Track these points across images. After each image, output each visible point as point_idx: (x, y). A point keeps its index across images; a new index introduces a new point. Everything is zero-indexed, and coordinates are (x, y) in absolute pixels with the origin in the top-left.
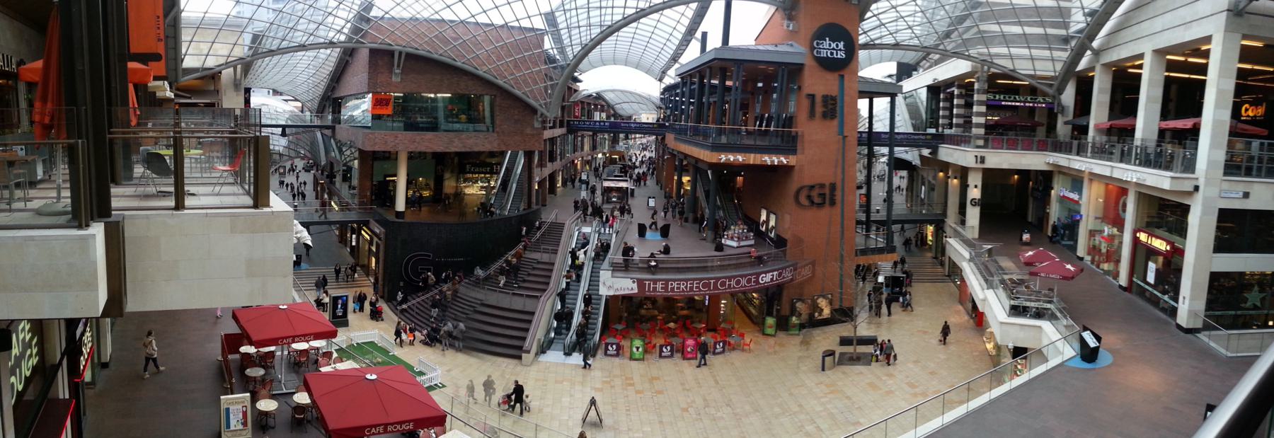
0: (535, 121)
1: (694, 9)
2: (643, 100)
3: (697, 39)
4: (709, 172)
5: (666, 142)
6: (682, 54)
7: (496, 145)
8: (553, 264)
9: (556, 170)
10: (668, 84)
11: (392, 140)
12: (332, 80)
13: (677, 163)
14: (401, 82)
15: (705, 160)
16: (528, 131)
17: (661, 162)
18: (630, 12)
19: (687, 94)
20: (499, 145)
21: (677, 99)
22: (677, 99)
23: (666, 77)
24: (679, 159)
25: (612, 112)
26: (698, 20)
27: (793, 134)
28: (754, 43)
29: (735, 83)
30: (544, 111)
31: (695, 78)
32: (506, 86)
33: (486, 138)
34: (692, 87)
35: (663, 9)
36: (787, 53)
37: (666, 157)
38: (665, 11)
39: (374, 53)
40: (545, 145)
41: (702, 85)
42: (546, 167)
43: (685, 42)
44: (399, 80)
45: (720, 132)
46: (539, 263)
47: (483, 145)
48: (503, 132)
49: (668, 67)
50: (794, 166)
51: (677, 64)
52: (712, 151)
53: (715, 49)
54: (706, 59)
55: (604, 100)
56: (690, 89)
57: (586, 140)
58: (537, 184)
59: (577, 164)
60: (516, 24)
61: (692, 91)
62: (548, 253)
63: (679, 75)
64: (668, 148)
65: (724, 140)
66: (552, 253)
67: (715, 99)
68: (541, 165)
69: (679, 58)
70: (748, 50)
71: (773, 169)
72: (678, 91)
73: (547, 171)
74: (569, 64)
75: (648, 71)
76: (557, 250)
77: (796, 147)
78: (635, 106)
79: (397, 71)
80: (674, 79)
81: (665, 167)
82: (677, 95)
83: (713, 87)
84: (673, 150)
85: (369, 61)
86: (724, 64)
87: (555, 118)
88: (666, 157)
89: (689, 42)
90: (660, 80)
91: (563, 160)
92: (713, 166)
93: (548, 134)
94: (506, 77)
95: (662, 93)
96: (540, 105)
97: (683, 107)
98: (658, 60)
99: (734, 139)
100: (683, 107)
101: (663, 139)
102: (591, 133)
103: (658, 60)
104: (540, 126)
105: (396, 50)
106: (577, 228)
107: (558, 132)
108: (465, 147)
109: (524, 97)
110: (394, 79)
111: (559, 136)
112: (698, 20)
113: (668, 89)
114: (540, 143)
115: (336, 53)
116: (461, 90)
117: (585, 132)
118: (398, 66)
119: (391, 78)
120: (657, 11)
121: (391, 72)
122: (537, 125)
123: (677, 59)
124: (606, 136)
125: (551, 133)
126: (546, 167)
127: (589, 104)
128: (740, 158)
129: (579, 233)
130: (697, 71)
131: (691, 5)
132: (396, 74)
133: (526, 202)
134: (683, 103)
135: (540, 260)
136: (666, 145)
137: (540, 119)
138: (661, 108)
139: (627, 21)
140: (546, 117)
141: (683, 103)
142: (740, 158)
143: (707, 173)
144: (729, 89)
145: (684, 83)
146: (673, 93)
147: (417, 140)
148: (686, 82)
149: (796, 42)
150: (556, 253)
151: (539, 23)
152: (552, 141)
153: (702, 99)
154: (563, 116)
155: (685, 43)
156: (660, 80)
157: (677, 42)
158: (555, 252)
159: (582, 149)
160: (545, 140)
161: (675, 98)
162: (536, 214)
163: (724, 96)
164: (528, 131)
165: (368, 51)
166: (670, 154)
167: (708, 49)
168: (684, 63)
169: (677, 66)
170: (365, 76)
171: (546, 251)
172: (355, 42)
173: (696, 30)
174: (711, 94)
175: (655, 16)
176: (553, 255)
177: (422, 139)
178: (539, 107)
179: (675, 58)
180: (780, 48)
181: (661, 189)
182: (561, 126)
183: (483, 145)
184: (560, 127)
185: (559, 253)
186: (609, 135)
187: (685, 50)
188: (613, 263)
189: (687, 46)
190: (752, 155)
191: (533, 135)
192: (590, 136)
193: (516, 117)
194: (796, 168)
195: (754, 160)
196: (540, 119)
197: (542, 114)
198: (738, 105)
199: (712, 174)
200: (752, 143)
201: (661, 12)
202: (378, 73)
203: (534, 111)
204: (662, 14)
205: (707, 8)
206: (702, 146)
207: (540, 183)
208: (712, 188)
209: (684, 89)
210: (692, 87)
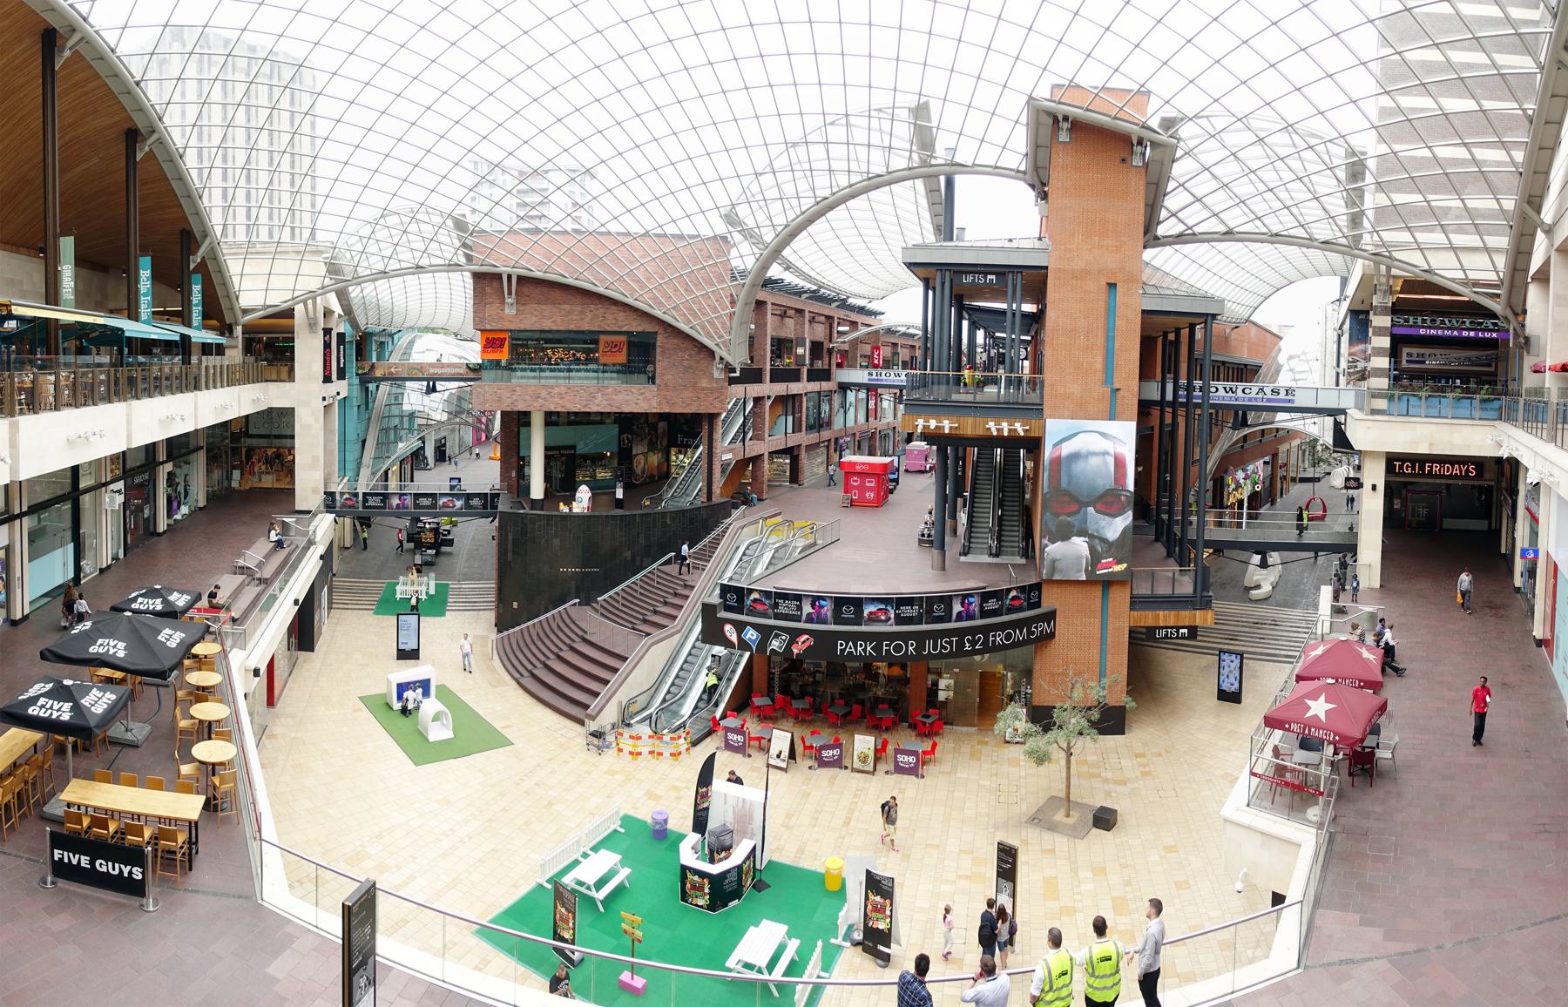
7: (655, 405)
11: (508, 395)
16: (704, 383)
30: (725, 354)
33: (642, 394)
47: (636, 404)
48: (666, 385)
60: (659, 231)
105: (505, 272)
110: (507, 310)
116: (608, 325)
118: (510, 293)
119: (503, 310)
121: (503, 302)
135: (687, 583)
147: (543, 395)
164: (704, 383)
177: (549, 393)
183: (636, 404)
191: (711, 390)
193: (686, 363)
197: (721, 359)
203: (711, 353)
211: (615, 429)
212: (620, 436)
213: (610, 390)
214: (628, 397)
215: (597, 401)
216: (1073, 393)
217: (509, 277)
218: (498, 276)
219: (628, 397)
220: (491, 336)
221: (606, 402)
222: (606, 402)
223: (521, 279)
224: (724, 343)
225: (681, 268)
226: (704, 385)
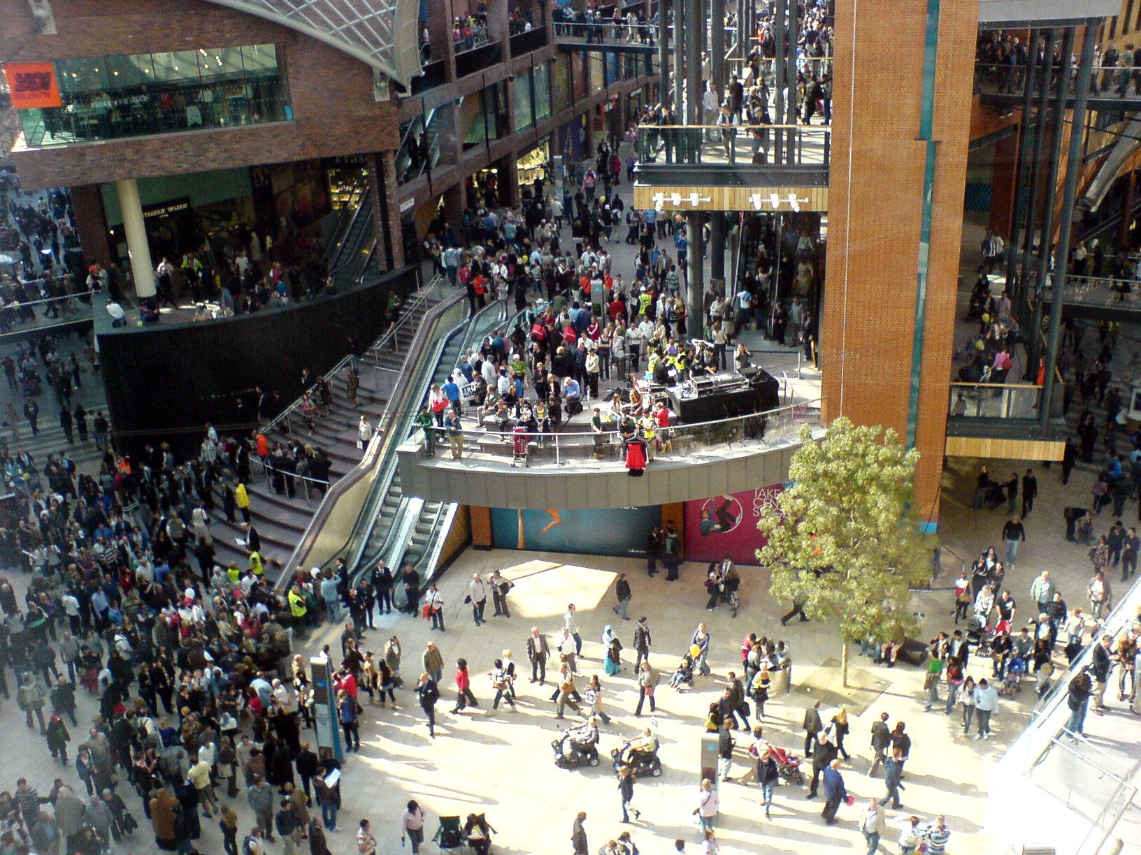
20: (303, 147)
33: (275, 136)
47: (269, 151)
96: (374, 56)
104: (387, 98)
137: (383, 84)
213: (227, 137)
215: (211, 155)
221: (224, 156)
222: (224, 156)
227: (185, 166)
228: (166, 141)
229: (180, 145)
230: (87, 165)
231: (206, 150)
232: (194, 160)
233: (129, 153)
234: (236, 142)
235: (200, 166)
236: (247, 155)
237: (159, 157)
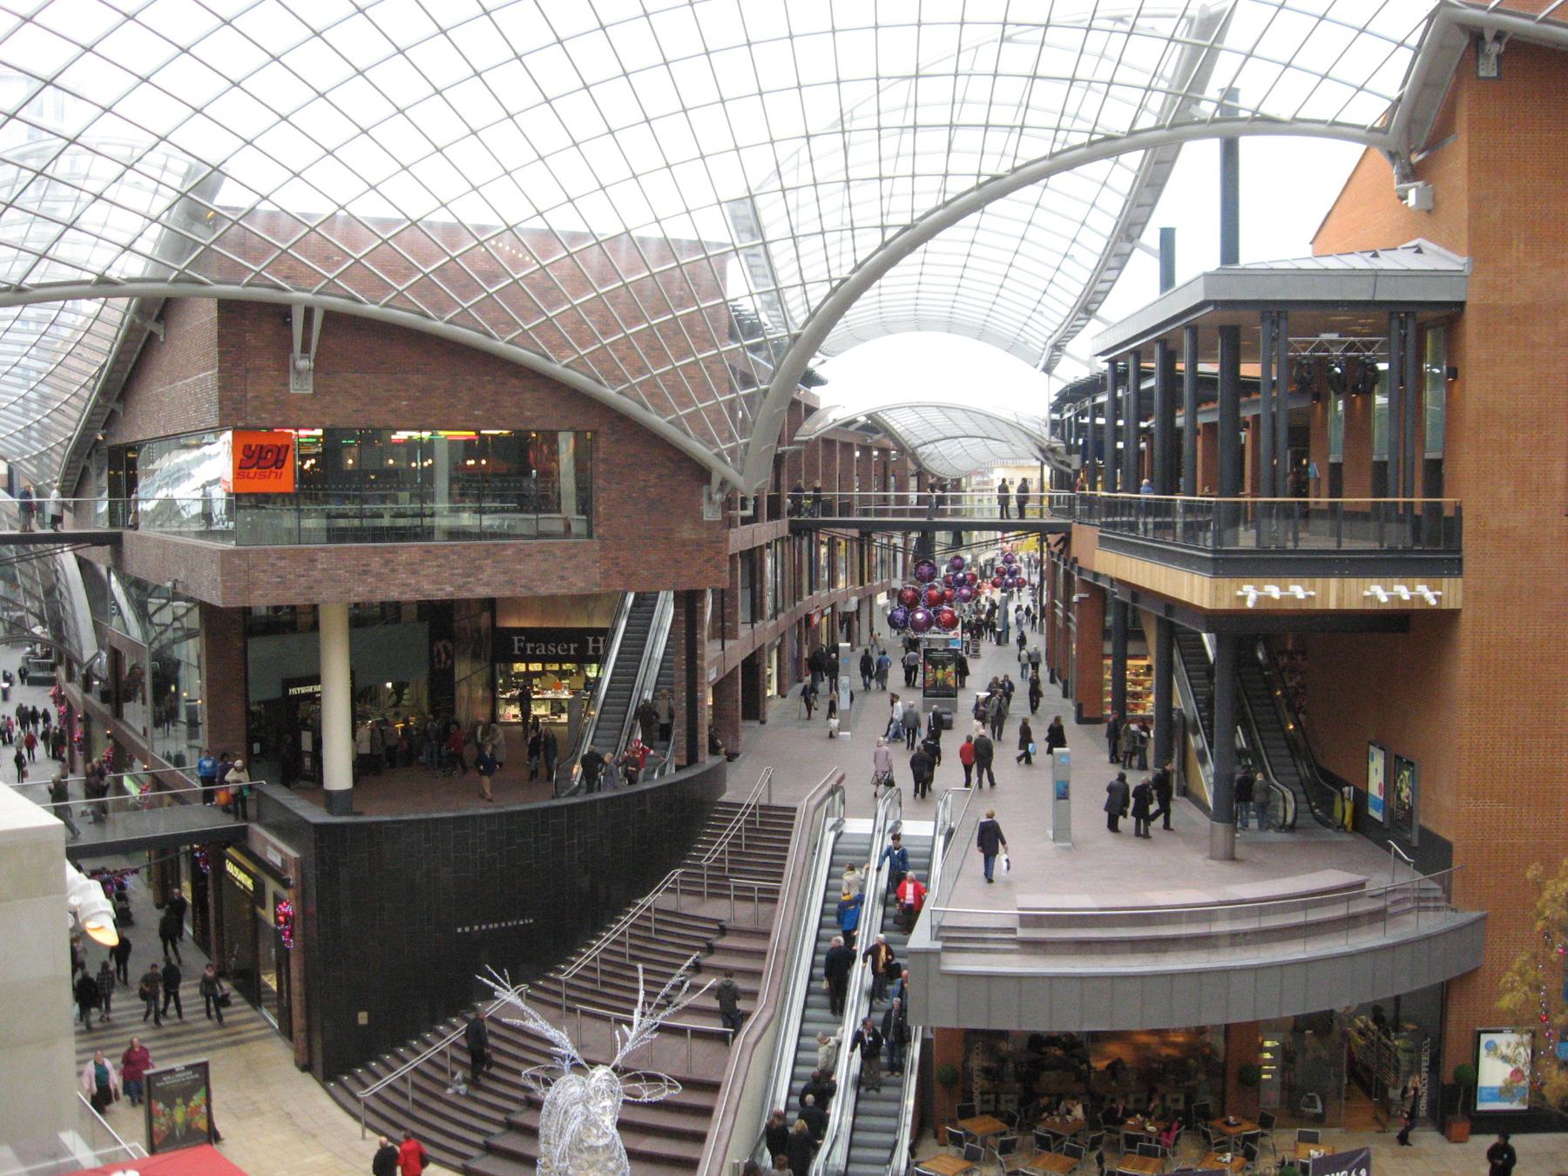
0: (705, 499)
1: (1136, 167)
2: (991, 428)
3: (1147, 249)
4: (1205, 637)
5: (1074, 553)
6: (1106, 293)
8: (766, 935)
9: (761, 649)
10: (1071, 380)
12: (104, 392)
13: (1110, 619)
14: (315, 394)
15: (1196, 602)
16: (686, 532)
17: (1060, 613)
18: (958, 185)
19: (1129, 407)
20: (606, 575)
21: (1100, 421)
22: (1100, 421)
23: (1064, 359)
24: (1118, 602)
25: (912, 467)
26: (1146, 199)
27: (1448, 512)
28: (1308, 250)
29: (1266, 371)
30: (731, 472)
31: (1150, 357)
32: (629, 405)
33: (571, 558)
34: (1144, 386)
35: (1047, 173)
36: (1409, 274)
37: (1075, 598)
38: (1053, 178)
39: (229, 308)
40: (733, 569)
41: (1171, 380)
42: (735, 637)
43: (1116, 257)
44: (309, 389)
45: (1236, 515)
46: (723, 931)
47: (562, 578)
49: (1070, 332)
50: (1460, 610)
51: (1093, 321)
52: (1216, 574)
53: (1206, 275)
54: (1179, 303)
55: (889, 433)
56: (1138, 393)
57: (841, 552)
58: (710, 692)
59: (818, 626)
61: (1143, 398)
62: (751, 899)
63: (1103, 354)
64: (1081, 570)
65: (1246, 539)
66: (761, 900)
67: (1214, 418)
68: (723, 631)
69: (1100, 303)
70: (1299, 273)
71: (1398, 621)
72: (1102, 399)
73: (737, 650)
74: (797, 337)
75: (1014, 347)
76: (777, 892)
77: (1459, 551)
78: (977, 448)
79: (304, 364)
80: (1088, 364)
81: (1073, 628)
82: (1098, 410)
83: (1204, 385)
84: (1096, 575)
85: (220, 336)
86: (1229, 317)
87: (757, 490)
88: (1075, 598)
89: (1124, 258)
90: (1048, 370)
91: (781, 616)
92: (1215, 620)
93: (740, 539)
94: (623, 380)
95: (1056, 408)
96: (719, 455)
97: (1120, 445)
98: (1041, 313)
99: (1280, 534)
100: (1120, 445)
101: (1066, 541)
102: (855, 533)
103: (1041, 313)
104: (719, 517)
105: (299, 302)
106: (831, 821)
107: (766, 531)
108: (511, 582)
109: (675, 434)
111: (768, 546)
112: (1146, 199)
113: (1074, 394)
114: (718, 569)
115: (117, 311)
117: (839, 530)
118: (305, 348)
119: (286, 385)
120: (1033, 179)
121: (284, 366)
122: (710, 514)
123: (1093, 307)
124: (898, 540)
125: (748, 536)
126: (735, 637)
127: (848, 447)
128: (1298, 591)
129: (838, 837)
130: (1157, 340)
131: (1123, 158)
132: (299, 372)
133: (683, 743)
134: (1118, 433)
136: (1076, 560)
138: (1053, 450)
139: (951, 214)
140: (735, 490)
141: (1118, 433)
142: (1298, 591)
143: (1201, 640)
144: (1251, 386)
145: (1119, 377)
146: (1088, 403)
148: (1126, 373)
149: (1430, 239)
150: (775, 901)
151: (715, 230)
152: (752, 558)
153: (1173, 417)
154: (777, 485)
155: (1113, 263)
156: (1048, 370)
157: (1092, 262)
158: (770, 896)
159: (832, 582)
160: (733, 557)
161: (1093, 419)
162: (714, 779)
163: (1236, 407)
164: (686, 532)
165: (213, 305)
166: (1087, 586)
167: (1181, 278)
168: (1115, 320)
169: (1093, 326)
170: (209, 376)
171: (744, 895)
172: (176, 281)
173: (1144, 224)
174: (1198, 401)
175: (1030, 192)
176: (765, 908)
178: (714, 462)
179: (1087, 308)
180: (1387, 262)
181: (1065, 695)
182: (774, 513)
184: (770, 518)
185: (783, 898)
186: (905, 536)
187: (1114, 282)
188: (942, 928)
189: (1120, 269)
190: (1333, 583)
192: (852, 539)
194: (1463, 616)
195: (1340, 599)
196: (718, 497)
197: (724, 483)
198: (1283, 436)
199: (1219, 646)
200: (1331, 545)
201: (1043, 182)
202: (247, 370)
203: (701, 473)
204: (1046, 186)
205: (1172, 162)
206: (1187, 562)
207: (718, 688)
208: (1221, 687)
209: (1120, 393)
210: (1144, 386)
211: (422, 630)
212: (432, 643)
214: (545, 566)
215: (484, 576)
216: (1515, 528)
217: (309, 312)
218: (282, 312)
219: (545, 566)
220: (255, 441)
221: (502, 578)
222: (502, 578)
223: (332, 317)
224: (732, 452)
225: (676, 306)
226: (686, 535)
227: (449, 589)
228: (427, 551)
229: (445, 557)
230: (316, 574)
231: (480, 569)
232: (460, 581)
233: (376, 563)
234: (520, 561)
235: (468, 590)
236: (532, 580)
237: (414, 572)
